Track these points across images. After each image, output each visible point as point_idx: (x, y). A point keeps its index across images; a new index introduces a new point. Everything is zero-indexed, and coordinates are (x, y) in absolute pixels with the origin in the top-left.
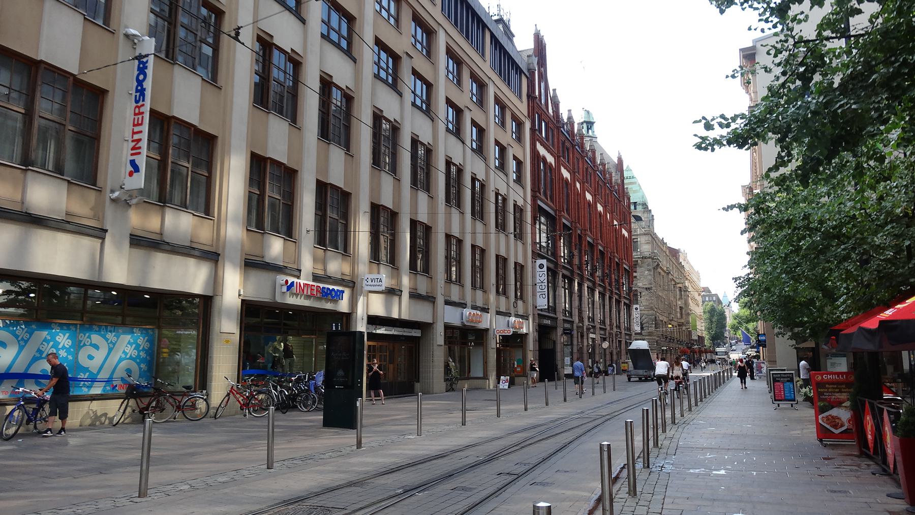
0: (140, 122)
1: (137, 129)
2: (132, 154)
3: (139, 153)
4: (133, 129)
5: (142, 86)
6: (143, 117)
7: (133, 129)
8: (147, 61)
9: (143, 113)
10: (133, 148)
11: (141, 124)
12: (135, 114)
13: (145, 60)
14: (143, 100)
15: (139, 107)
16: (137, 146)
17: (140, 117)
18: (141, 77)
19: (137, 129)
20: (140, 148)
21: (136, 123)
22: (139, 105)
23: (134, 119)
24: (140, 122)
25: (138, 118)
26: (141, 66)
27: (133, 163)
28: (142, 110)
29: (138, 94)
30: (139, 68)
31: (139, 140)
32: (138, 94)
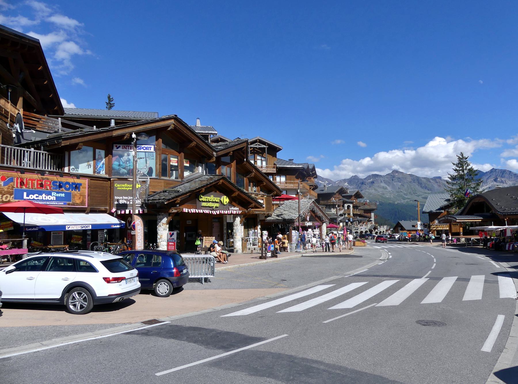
3: (122, 149)
5: (142, 149)
8: (149, 150)
13: (149, 149)
16: (125, 148)
18: (144, 148)
20: (124, 149)
21: (131, 147)
26: (148, 148)
29: (140, 148)
32: (140, 148)
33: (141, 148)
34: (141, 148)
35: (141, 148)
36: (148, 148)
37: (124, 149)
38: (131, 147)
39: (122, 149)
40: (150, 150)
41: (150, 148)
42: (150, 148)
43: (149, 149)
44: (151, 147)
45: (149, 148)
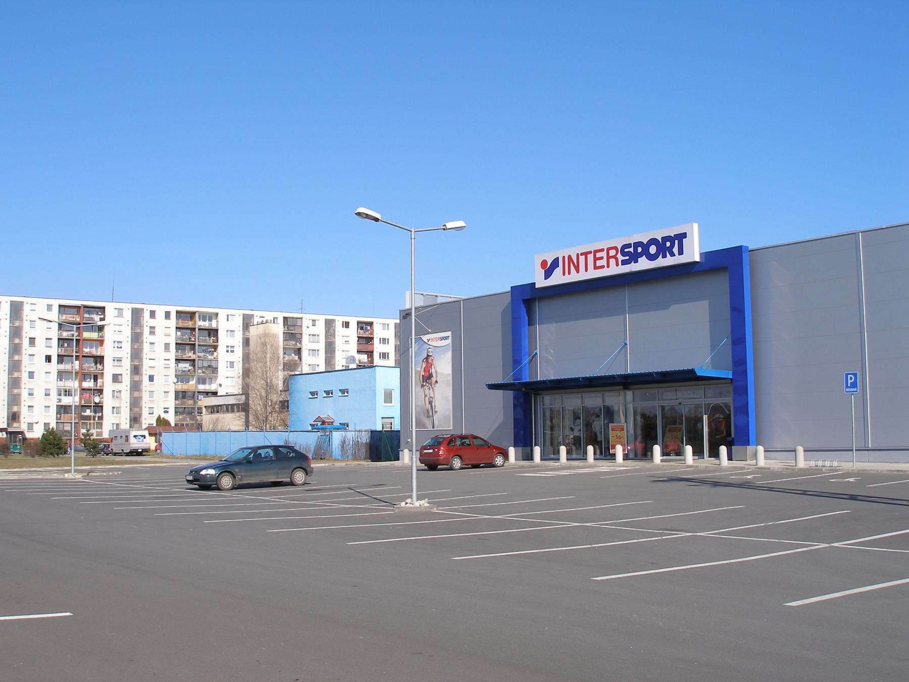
0: (599, 263)
1: (591, 257)
2: (564, 257)
3: (564, 274)
4: (590, 252)
5: (640, 255)
6: (603, 267)
7: (590, 252)
8: (672, 255)
9: (608, 266)
10: (570, 257)
11: (596, 268)
12: (609, 249)
13: (675, 250)
14: (624, 263)
15: (615, 257)
17: (605, 260)
19: (591, 257)
20: (569, 273)
21: (598, 255)
22: (620, 258)
23: (602, 250)
24: (599, 263)
25: (602, 258)
26: (668, 244)
27: (555, 263)
28: (612, 261)
29: (631, 250)
30: (665, 239)
31: (577, 270)
32: (631, 250)
33: (640, 250)
34: (640, 250)
35: (635, 249)
36: (668, 244)
37: (569, 273)
38: (598, 255)
39: (564, 274)
40: (681, 252)
41: (676, 241)
42: (676, 241)
43: (675, 250)
44: (684, 235)
45: (673, 245)
